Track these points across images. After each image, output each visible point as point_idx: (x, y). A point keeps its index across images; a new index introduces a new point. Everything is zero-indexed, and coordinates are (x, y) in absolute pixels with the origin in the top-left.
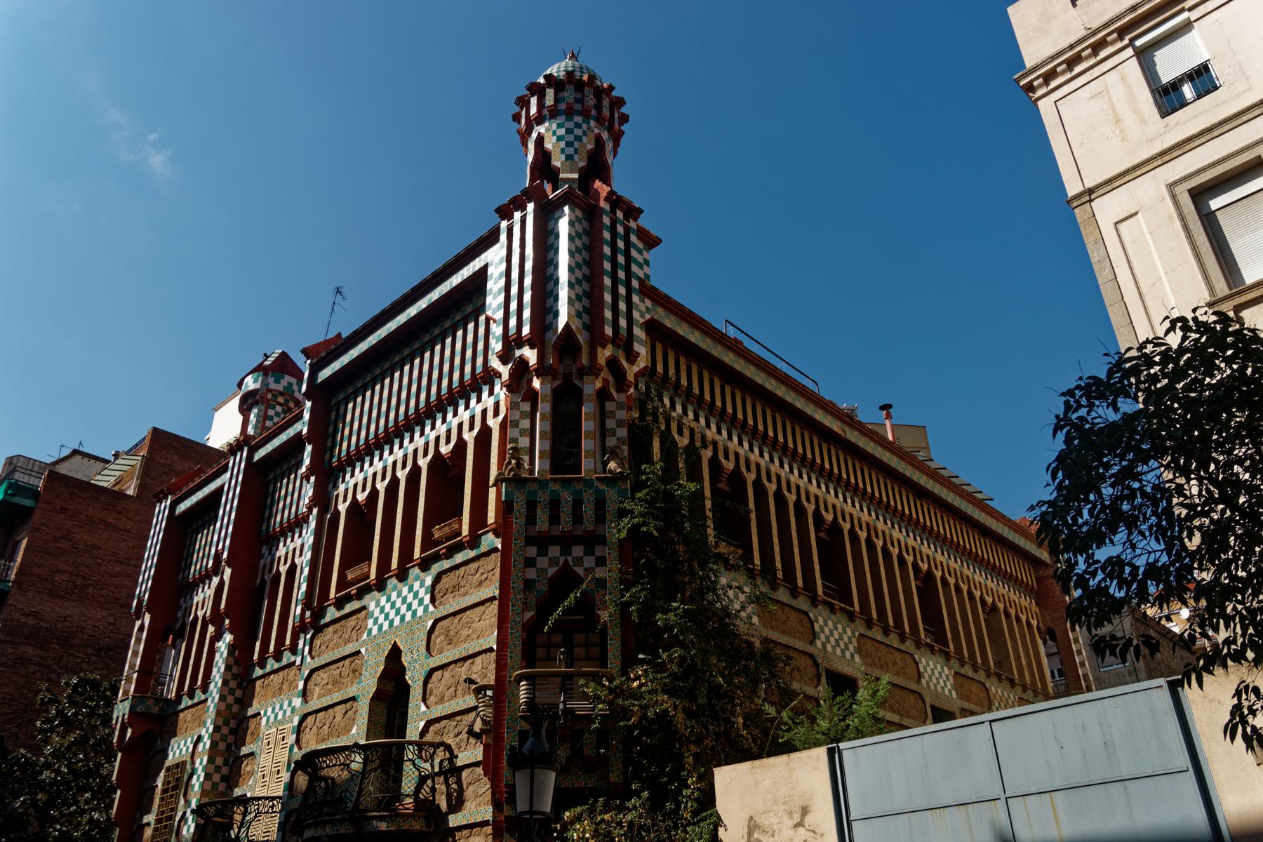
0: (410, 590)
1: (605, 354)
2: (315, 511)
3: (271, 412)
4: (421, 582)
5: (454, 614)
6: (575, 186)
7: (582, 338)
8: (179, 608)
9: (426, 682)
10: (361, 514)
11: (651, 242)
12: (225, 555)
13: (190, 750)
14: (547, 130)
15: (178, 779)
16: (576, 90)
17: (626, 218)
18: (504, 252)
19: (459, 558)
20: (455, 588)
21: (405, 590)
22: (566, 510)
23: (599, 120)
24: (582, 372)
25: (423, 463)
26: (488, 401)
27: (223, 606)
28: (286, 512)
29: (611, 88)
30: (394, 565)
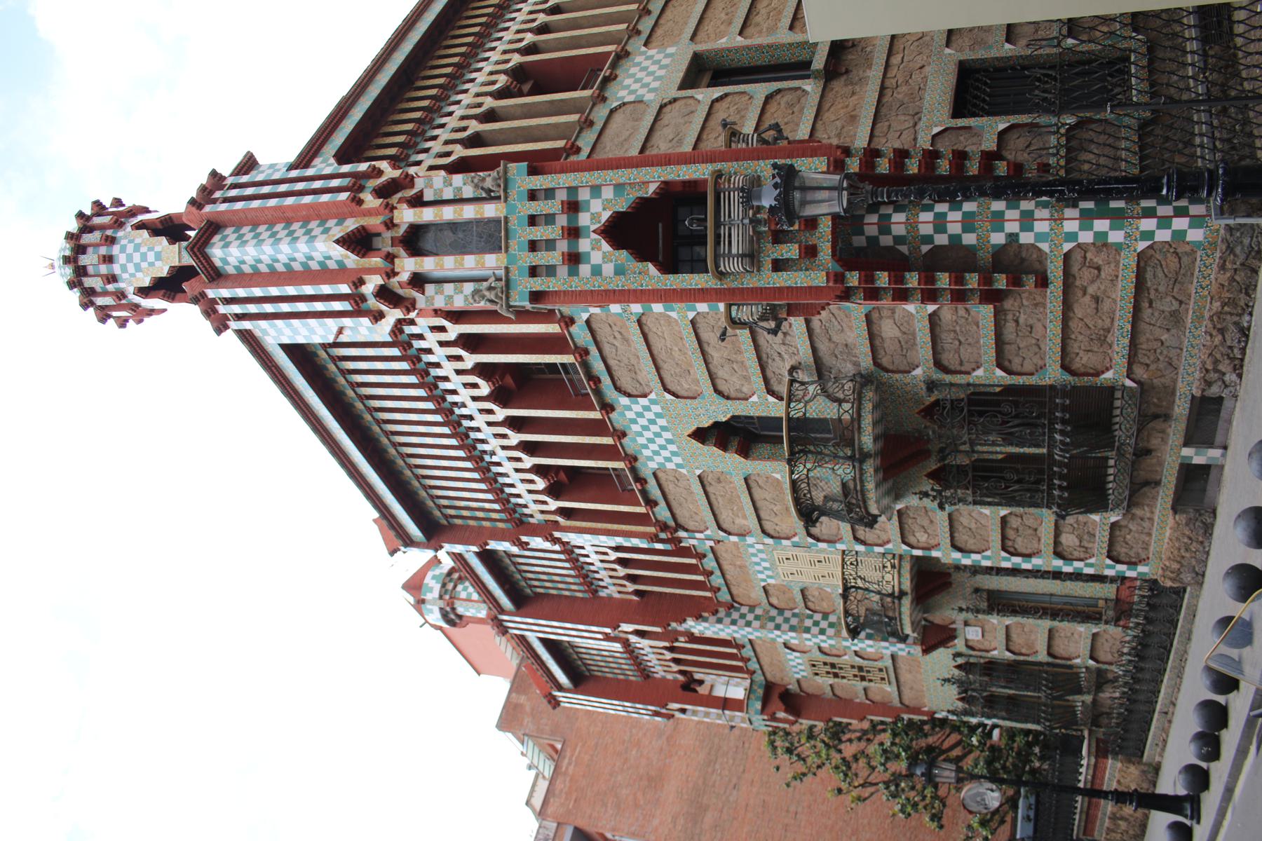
0: (634, 421)
1: (370, 201)
2: (557, 534)
3: (463, 595)
4: (628, 412)
5: (658, 369)
6: (184, 244)
7: (351, 225)
8: (664, 679)
10: (562, 483)
11: (249, 164)
12: (608, 630)
13: (798, 654)
14: (130, 283)
15: (825, 664)
16: (84, 253)
17: (221, 188)
18: (263, 324)
19: (598, 367)
20: (633, 370)
21: (635, 428)
22: (539, 233)
23: (118, 224)
24: (390, 224)
25: (501, 414)
26: (431, 340)
27: (658, 630)
28: (573, 587)
29: (80, 215)
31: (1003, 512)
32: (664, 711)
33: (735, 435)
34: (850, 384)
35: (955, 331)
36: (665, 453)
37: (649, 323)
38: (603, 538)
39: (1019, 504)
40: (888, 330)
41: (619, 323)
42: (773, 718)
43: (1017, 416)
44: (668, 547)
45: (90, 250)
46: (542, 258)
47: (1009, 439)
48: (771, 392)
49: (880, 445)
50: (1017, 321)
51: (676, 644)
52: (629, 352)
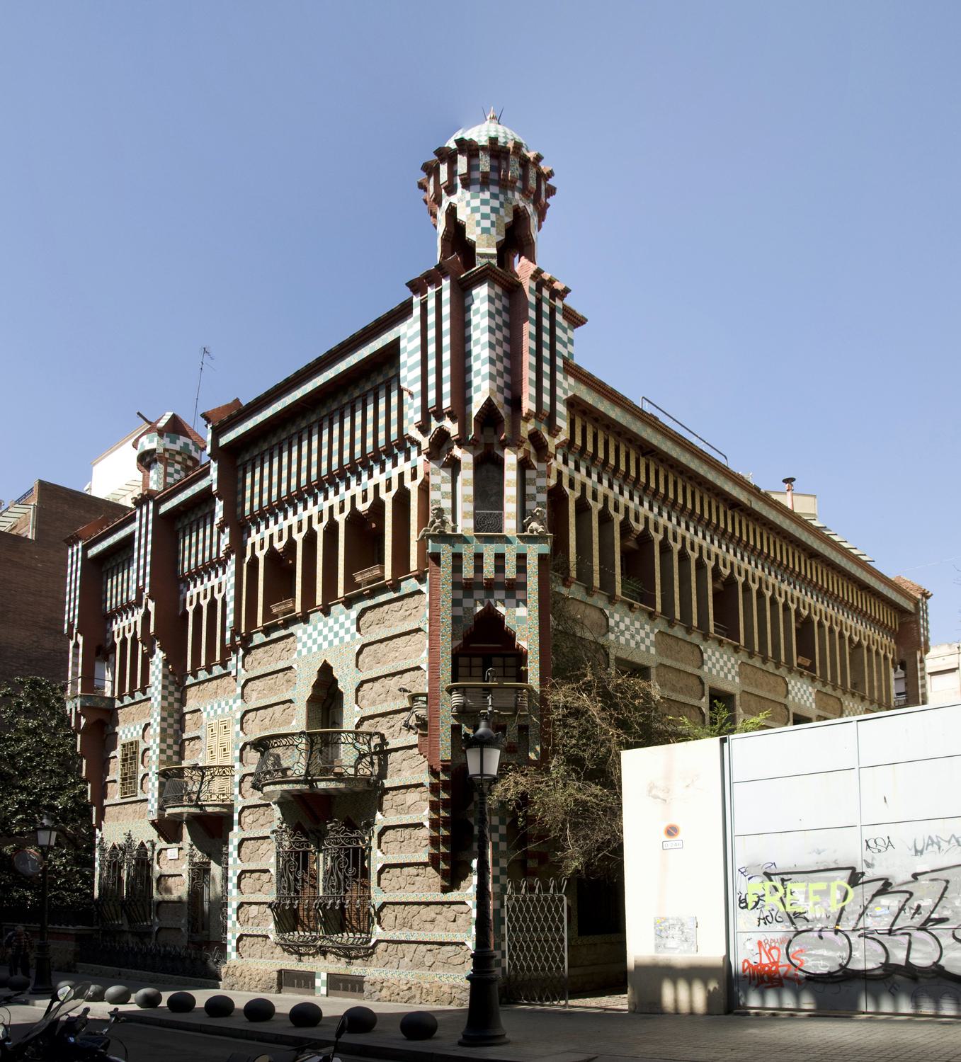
0: (336, 621)
4: (343, 617)
9: (358, 690)
10: (279, 563)
20: (380, 622)
27: (152, 629)
30: (319, 601)
31: (273, 871)
32: (75, 631)
33: (327, 694)
34: (369, 773)
35: (410, 838)
36: (310, 643)
37: (419, 636)
38: (232, 593)
39: (279, 881)
40: (412, 796)
41: (418, 614)
42: (78, 716)
43: (345, 877)
44: (228, 642)
47: (329, 873)
48: (363, 720)
49: (322, 793)
50: (418, 875)
51: (140, 645)
52: (396, 618)
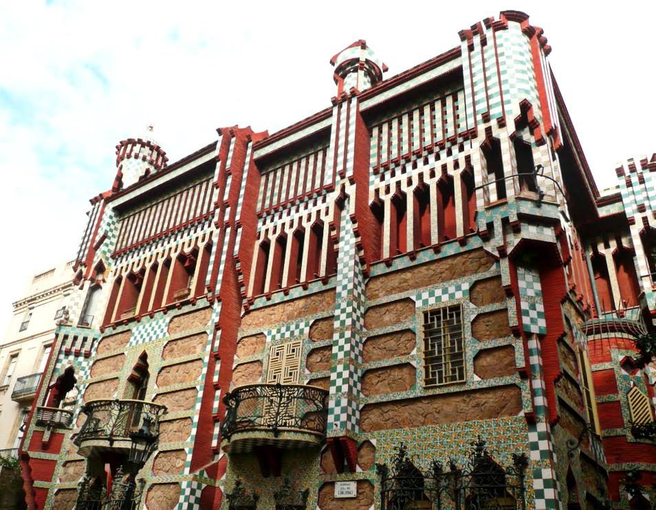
45: (150, 152)
46: (69, 341)
